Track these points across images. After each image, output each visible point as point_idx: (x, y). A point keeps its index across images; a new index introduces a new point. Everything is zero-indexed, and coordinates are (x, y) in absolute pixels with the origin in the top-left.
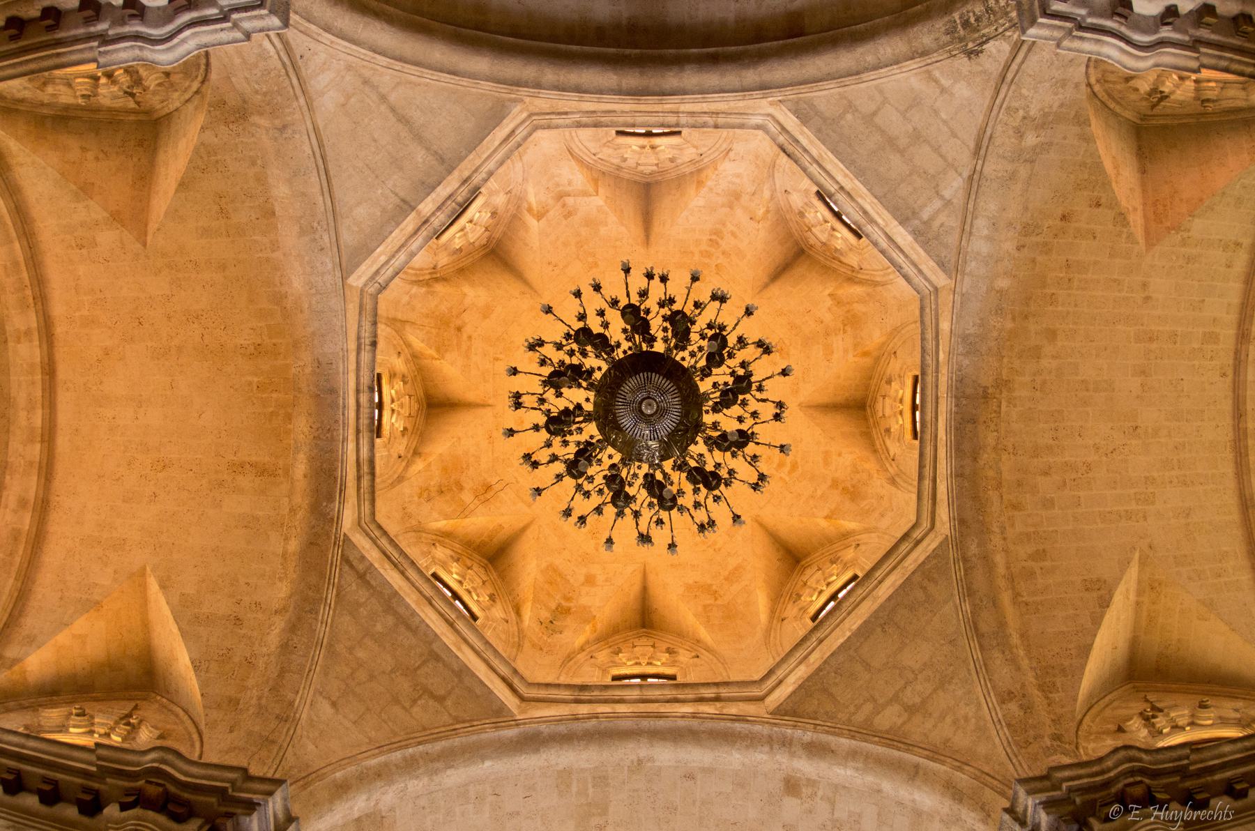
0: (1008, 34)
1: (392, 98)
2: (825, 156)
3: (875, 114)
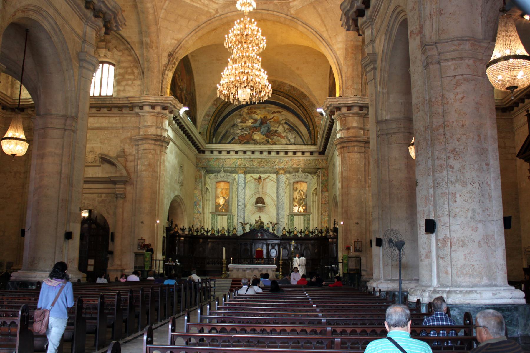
0: (165, 68)
1: (324, 29)
2: (199, 2)
3: (188, 22)
